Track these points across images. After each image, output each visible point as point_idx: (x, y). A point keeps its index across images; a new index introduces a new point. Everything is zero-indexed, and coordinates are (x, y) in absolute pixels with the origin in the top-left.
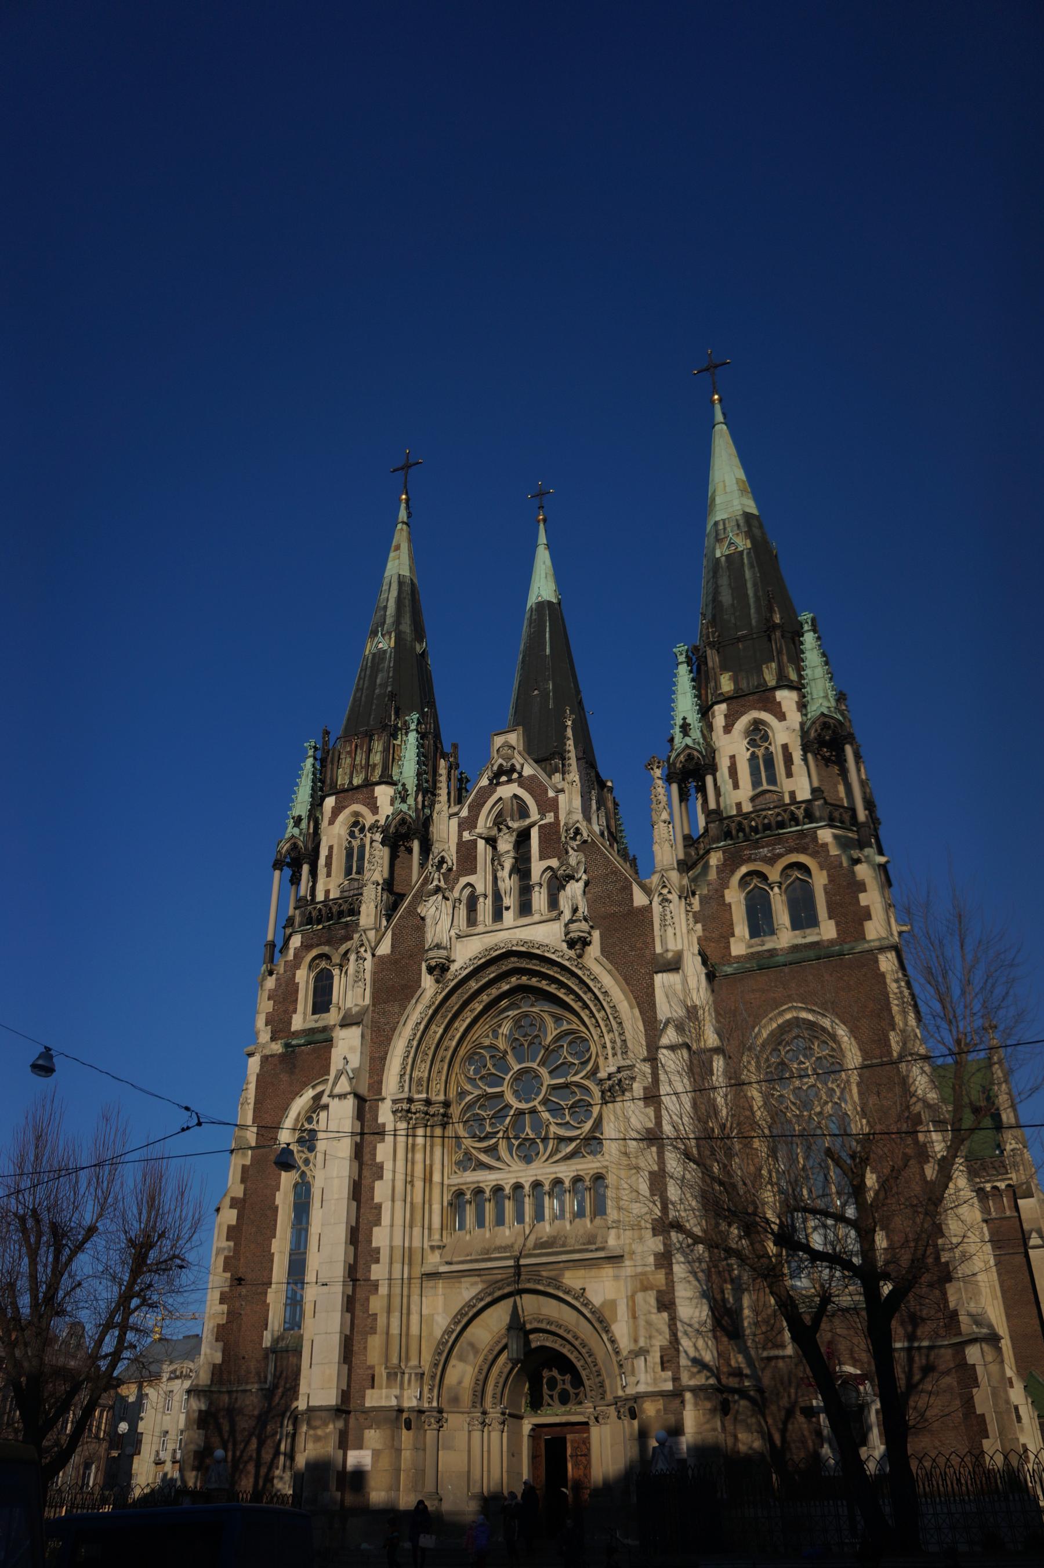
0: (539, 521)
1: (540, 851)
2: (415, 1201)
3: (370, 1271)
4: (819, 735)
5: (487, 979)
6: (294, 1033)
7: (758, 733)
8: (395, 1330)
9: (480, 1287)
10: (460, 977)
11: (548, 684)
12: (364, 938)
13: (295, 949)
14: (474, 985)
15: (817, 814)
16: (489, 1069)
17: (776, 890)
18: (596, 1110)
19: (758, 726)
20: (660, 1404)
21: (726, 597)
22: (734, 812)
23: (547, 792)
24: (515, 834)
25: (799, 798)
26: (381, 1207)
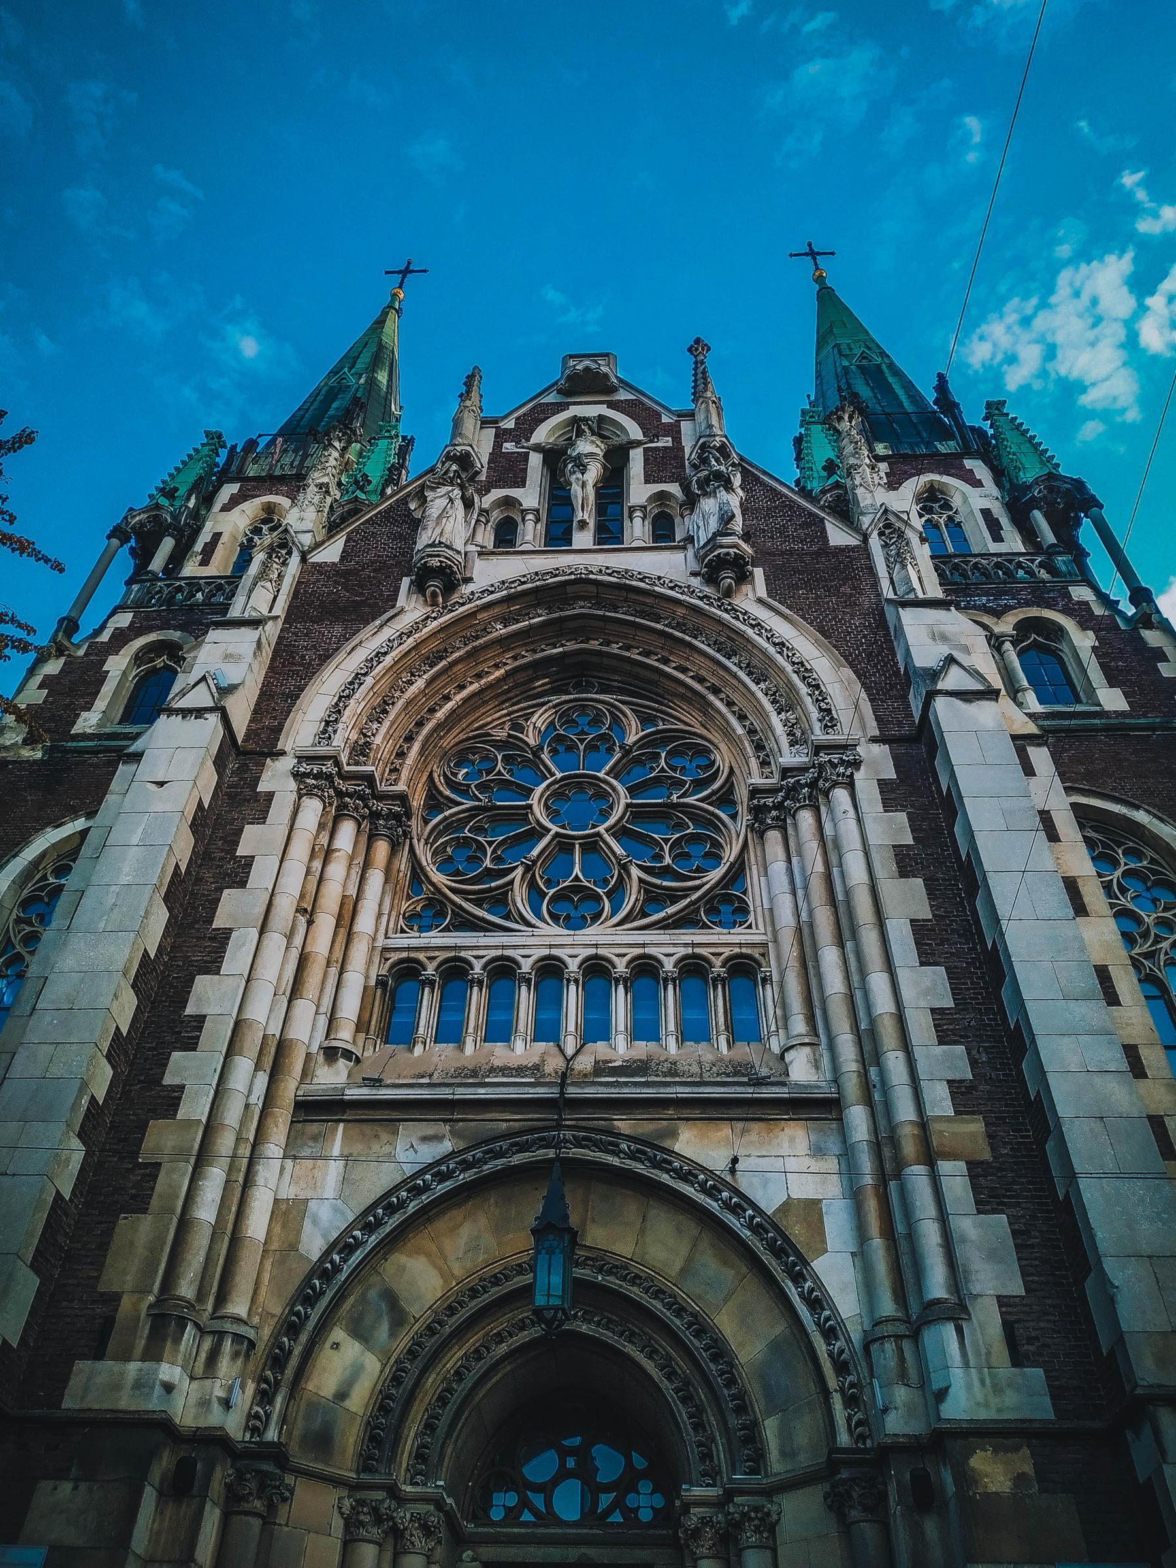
2: (308, 949)
3: (166, 1065)
6: (77, 735)
9: (447, 1146)
13: (116, 629)
16: (499, 773)
17: (1008, 646)
18: (730, 854)
26: (228, 938)
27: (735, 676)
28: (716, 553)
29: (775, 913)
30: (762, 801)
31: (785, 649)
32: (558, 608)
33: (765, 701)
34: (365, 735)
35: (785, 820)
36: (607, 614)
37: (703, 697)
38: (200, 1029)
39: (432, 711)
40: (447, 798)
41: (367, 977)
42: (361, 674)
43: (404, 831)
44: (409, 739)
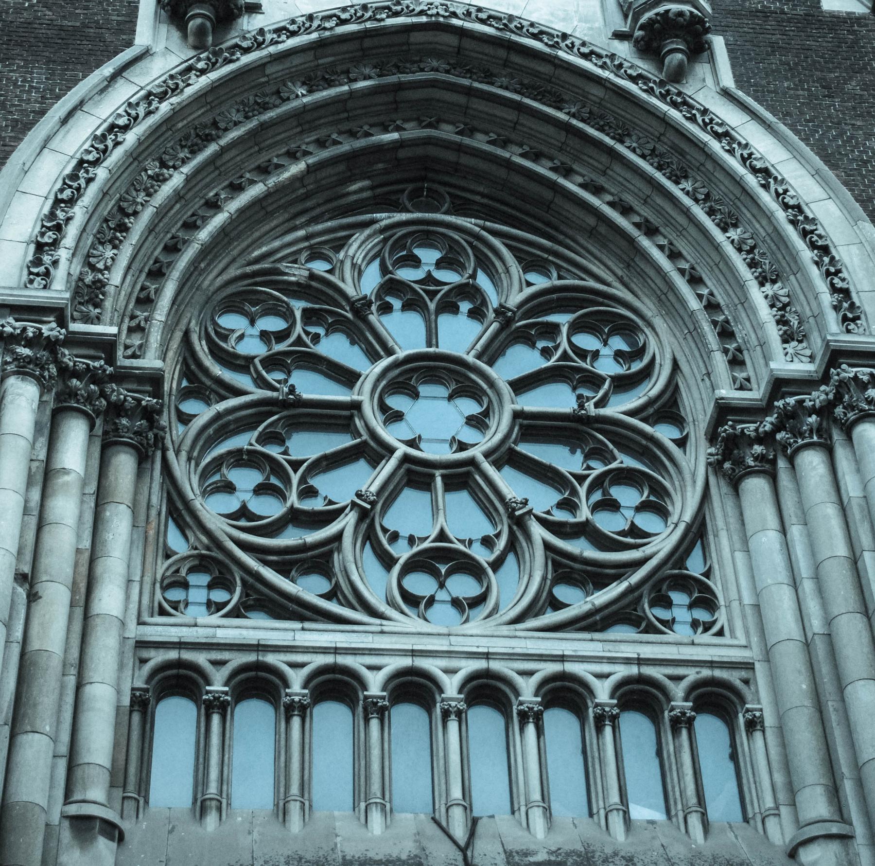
5: (346, 88)
10: (272, 49)
27: (686, 213)
28: (661, 9)
29: (766, 611)
30: (739, 427)
31: (771, 180)
32: (398, 67)
33: (738, 261)
34: (93, 267)
35: (774, 462)
36: (476, 85)
37: (631, 241)
39: (192, 226)
40: (219, 381)
41: (119, 692)
42: (88, 162)
43: (156, 436)
44: (157, 273)
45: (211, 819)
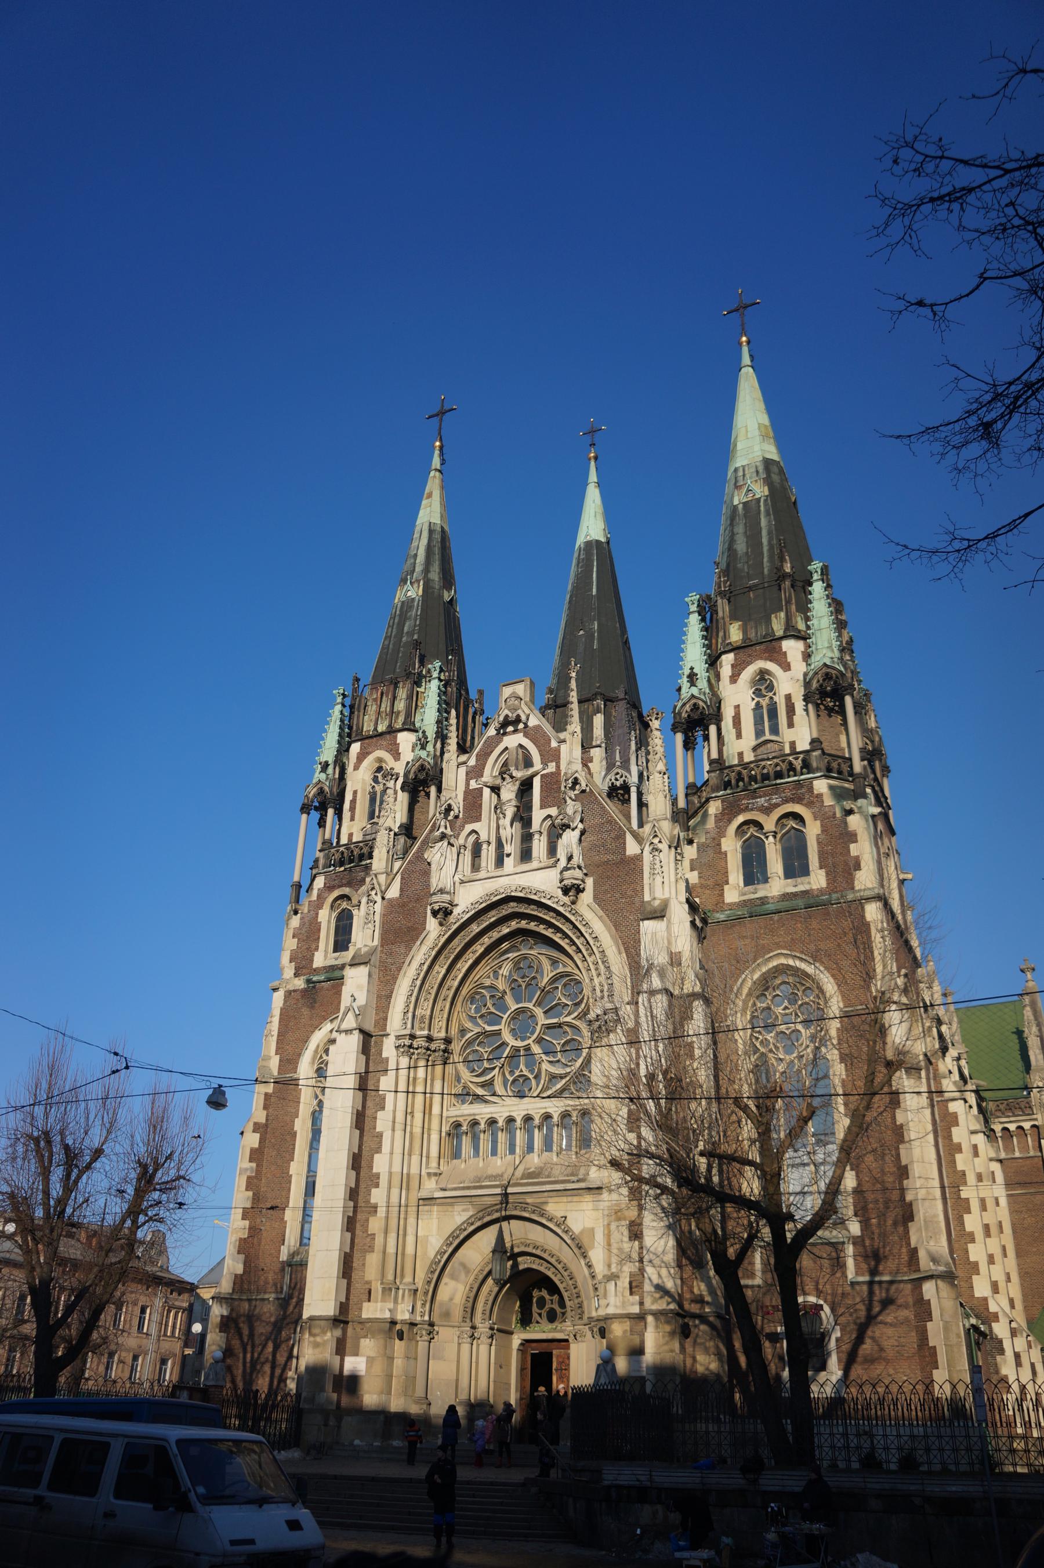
0: (590, 459)
1: (541, 800)
4: (821, 686)
7: (763, 683)
8: (391, 1249)
9: (471, 1213)
10: (462, 921)
11: (593, 624)
12: (375, 881)
14: (475, 928)
15: (814, 765)
17: (771, 839)
19: (763, 674)
20: (627, 1325)
21: (741, 546)
22: (736, 762)
23: (550, 743)
24: (518, 783)
25: (798, 749)
38: (378, 1178)
45: (463, 1166)
